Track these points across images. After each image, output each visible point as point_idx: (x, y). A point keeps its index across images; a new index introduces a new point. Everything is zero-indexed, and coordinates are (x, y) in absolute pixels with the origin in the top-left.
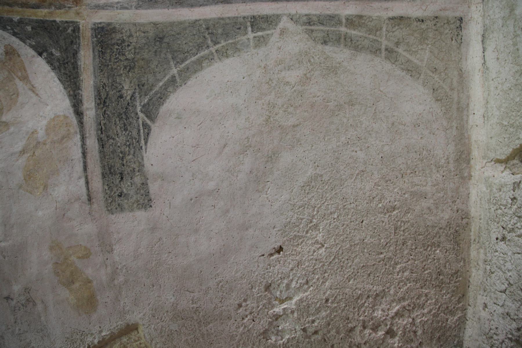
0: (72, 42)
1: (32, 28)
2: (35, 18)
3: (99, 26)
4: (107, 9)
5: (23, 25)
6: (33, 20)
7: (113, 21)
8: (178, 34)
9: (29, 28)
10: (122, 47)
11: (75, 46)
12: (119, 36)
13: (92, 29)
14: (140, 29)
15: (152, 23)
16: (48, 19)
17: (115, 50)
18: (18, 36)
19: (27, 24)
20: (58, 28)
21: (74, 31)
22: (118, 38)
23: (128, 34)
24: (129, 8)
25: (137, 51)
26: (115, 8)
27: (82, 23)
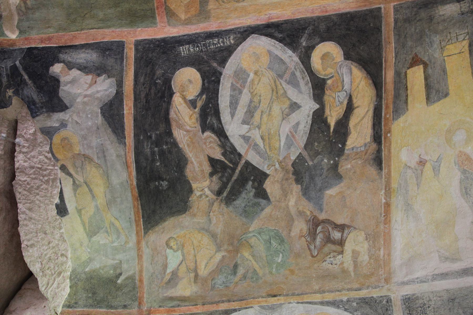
0: (387, 309)
1: (357, 304)
2: (358, 297)
3: (406, 297)
4: (410, 284)
5: (350, 303)
6: (356, 298)
7: (416, 292)
8: (466, 296)
9: (355, 304)
10: (424, 308)
11: (389, 312)
12: (421, 301)
13: (401, 300)
14: (437, 295)
15: (445, 290)
16: (367, 296)
17: (419, 311)
18: (348, 311)
19: (353, 302)
20: (376, 301)
21: (387, 302)
22: (420, 303)
23: (428, 299)
24: (427, 281)
25: (436, 310)
26: (416, 283)
27: (392, 296)
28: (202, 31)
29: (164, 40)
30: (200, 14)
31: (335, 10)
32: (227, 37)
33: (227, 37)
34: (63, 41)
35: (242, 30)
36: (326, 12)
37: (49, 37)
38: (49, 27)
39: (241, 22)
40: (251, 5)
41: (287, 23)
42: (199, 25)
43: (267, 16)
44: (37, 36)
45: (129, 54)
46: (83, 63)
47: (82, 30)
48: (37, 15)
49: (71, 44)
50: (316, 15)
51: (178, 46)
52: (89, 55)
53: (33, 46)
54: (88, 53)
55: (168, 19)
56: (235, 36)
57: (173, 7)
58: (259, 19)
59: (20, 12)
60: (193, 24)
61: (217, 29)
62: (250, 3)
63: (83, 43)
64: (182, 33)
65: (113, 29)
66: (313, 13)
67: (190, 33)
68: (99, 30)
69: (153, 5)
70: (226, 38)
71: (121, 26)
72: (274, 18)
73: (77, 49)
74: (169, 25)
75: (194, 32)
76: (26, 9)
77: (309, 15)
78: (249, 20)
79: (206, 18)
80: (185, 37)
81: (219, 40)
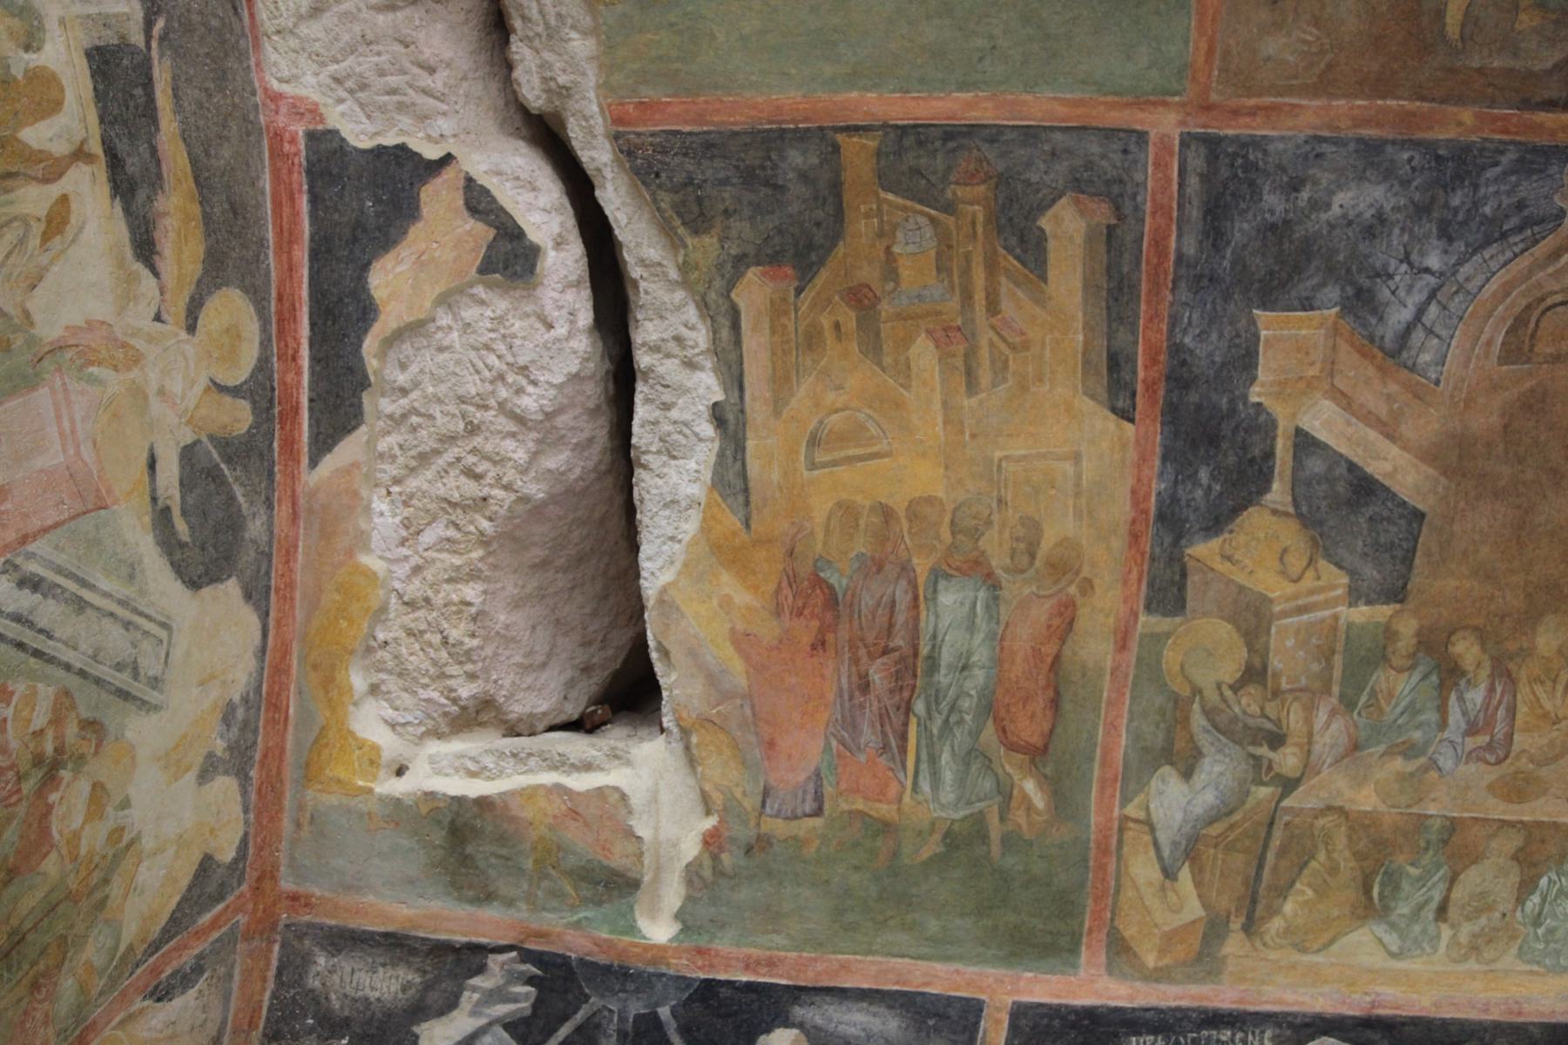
28: (1195, 1004)
29: (1090, 1013)
30: (1199, 957)
31: (1542, 1014)
32: (1257, 1031)
33: (1257, 1031)
34: (810, 974)
35: (1298, 1021)
36: (1520, 1014)
37: (771, 957)
38: (775, 931)
39: (1301, 999)
40: (1332, 964)
41: (1415, 1025)
42: (1190, 987)
43: (1368, 999)
44: (734, 950)
45: (991, 1035)
46: (858, 1038)
47: (870, 952)
48: (744, 894)
49: (832, 984)
50: (1491, 1018)
51: (1128, 1035)
52: (877, 1021)
53: (722, 977)
54: (875, 1015)
55: (1108, 958)
56: (1277, 1031)
57: (1130, 932)
58: (1348, 1001)
59: (696, 880)
60: (1171, 980)
61: (1234, 1006)
62: (1333, 960)
63: (865, 986)
64: (1140, 1002)
65: (960, 966)
66: (1486, 1011)
67: (1163, 1004)
68: (920, 962)
69: (1081, 924)
70: (1253, 1033)
71: (981, 960)
72: (1384, 1007)
73: (847, 998)
74: (1110, 972)
75: (1173, 1004)
76: (714, 873)
77: (1474, 1015)
78: (1321, 999)
79: (1209, 973)
80: (1148, 1015)
81: (1234, 1035)
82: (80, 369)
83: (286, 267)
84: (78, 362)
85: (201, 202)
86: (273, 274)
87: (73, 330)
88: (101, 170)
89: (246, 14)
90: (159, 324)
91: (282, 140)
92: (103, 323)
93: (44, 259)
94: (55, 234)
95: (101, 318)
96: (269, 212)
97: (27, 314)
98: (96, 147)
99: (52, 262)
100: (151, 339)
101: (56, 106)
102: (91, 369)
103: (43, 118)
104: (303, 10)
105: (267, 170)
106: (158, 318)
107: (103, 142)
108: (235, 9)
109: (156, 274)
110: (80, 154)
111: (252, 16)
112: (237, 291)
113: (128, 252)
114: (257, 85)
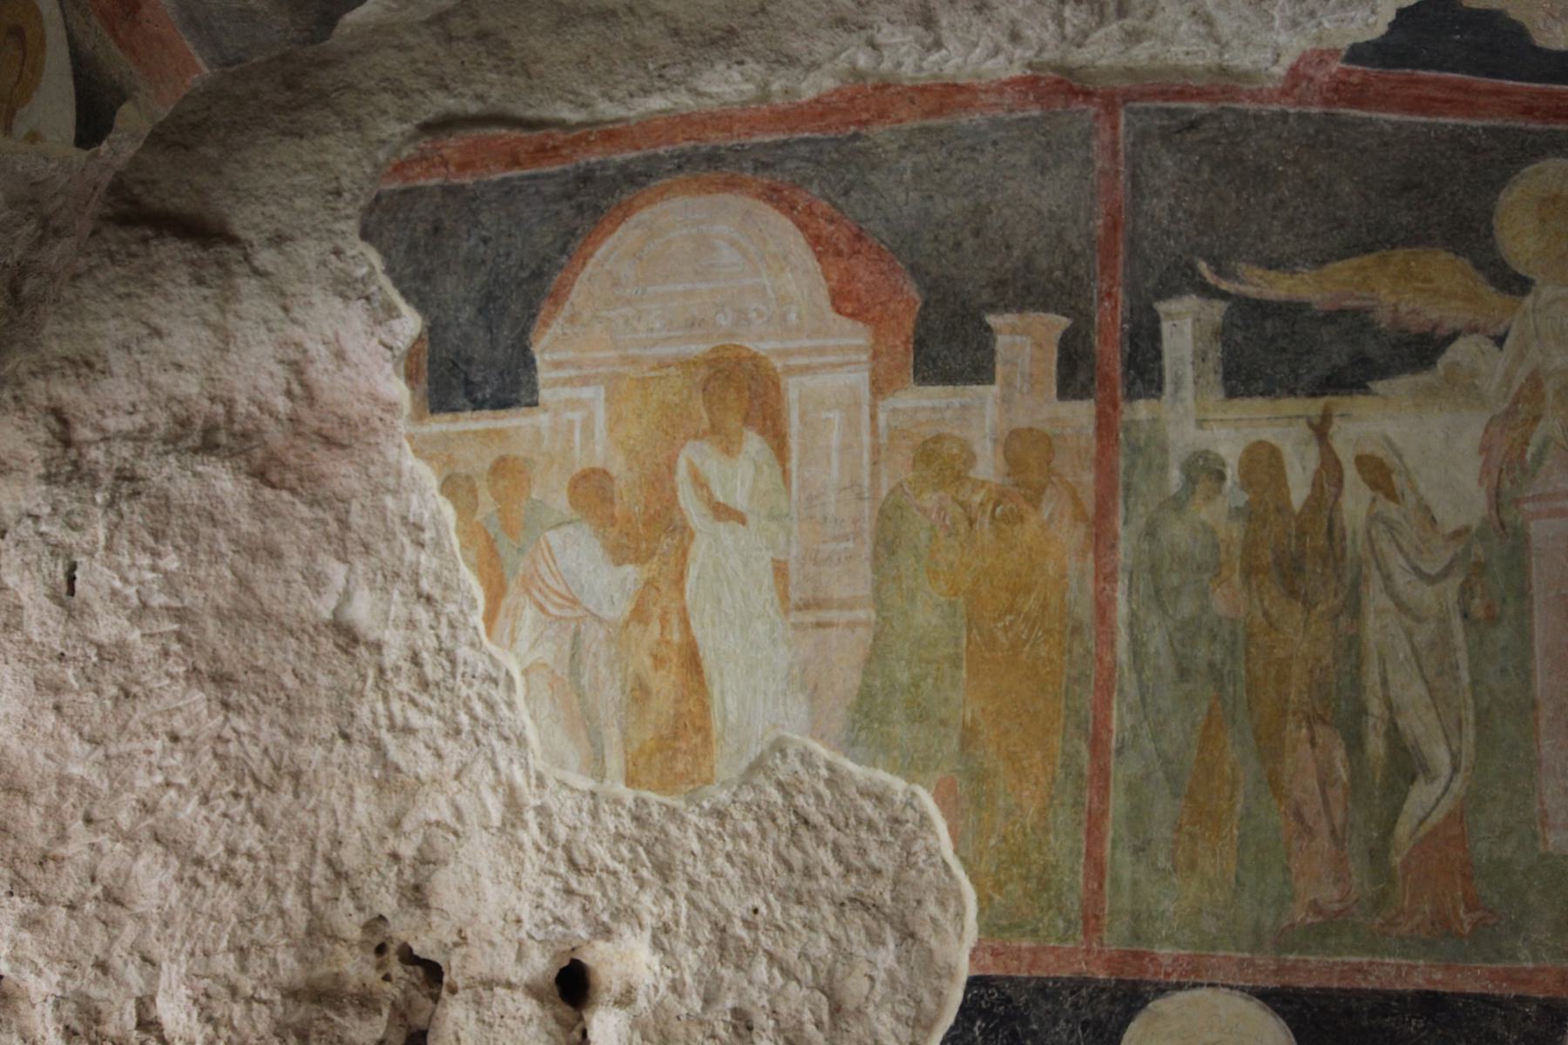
82: (1524, 471)
83: (1494, 99)
84: (1517, 473)
85: (1394, 247)
86: (1497, 122)
87: (1485, 471)
88: (1341, 403)
89: (1199, 106)
90: (1509, 342)
91: (1344, 83)
92: (1486, 431)
93: (1410, 499)
94: (1391, 483)
95: (1481, 432)
96: (1423, 119)
97: (1458, 534)
98: (1315, 407)
99: (1415, 490)
100: (1521, 356)
101: (1274, 453)
102: (1528, 456)
103: (1284, 475)
104: (1202, 30)
105: (1375, 115)
106: (1500, 341)
107: (1313, 395)
108: (1193, 126)
109: (1453, 336)
110: (1321, 431)
111: (1200, 94)
112: (1501, 197)
113: (1424, 378)
114: (1275, 107)
